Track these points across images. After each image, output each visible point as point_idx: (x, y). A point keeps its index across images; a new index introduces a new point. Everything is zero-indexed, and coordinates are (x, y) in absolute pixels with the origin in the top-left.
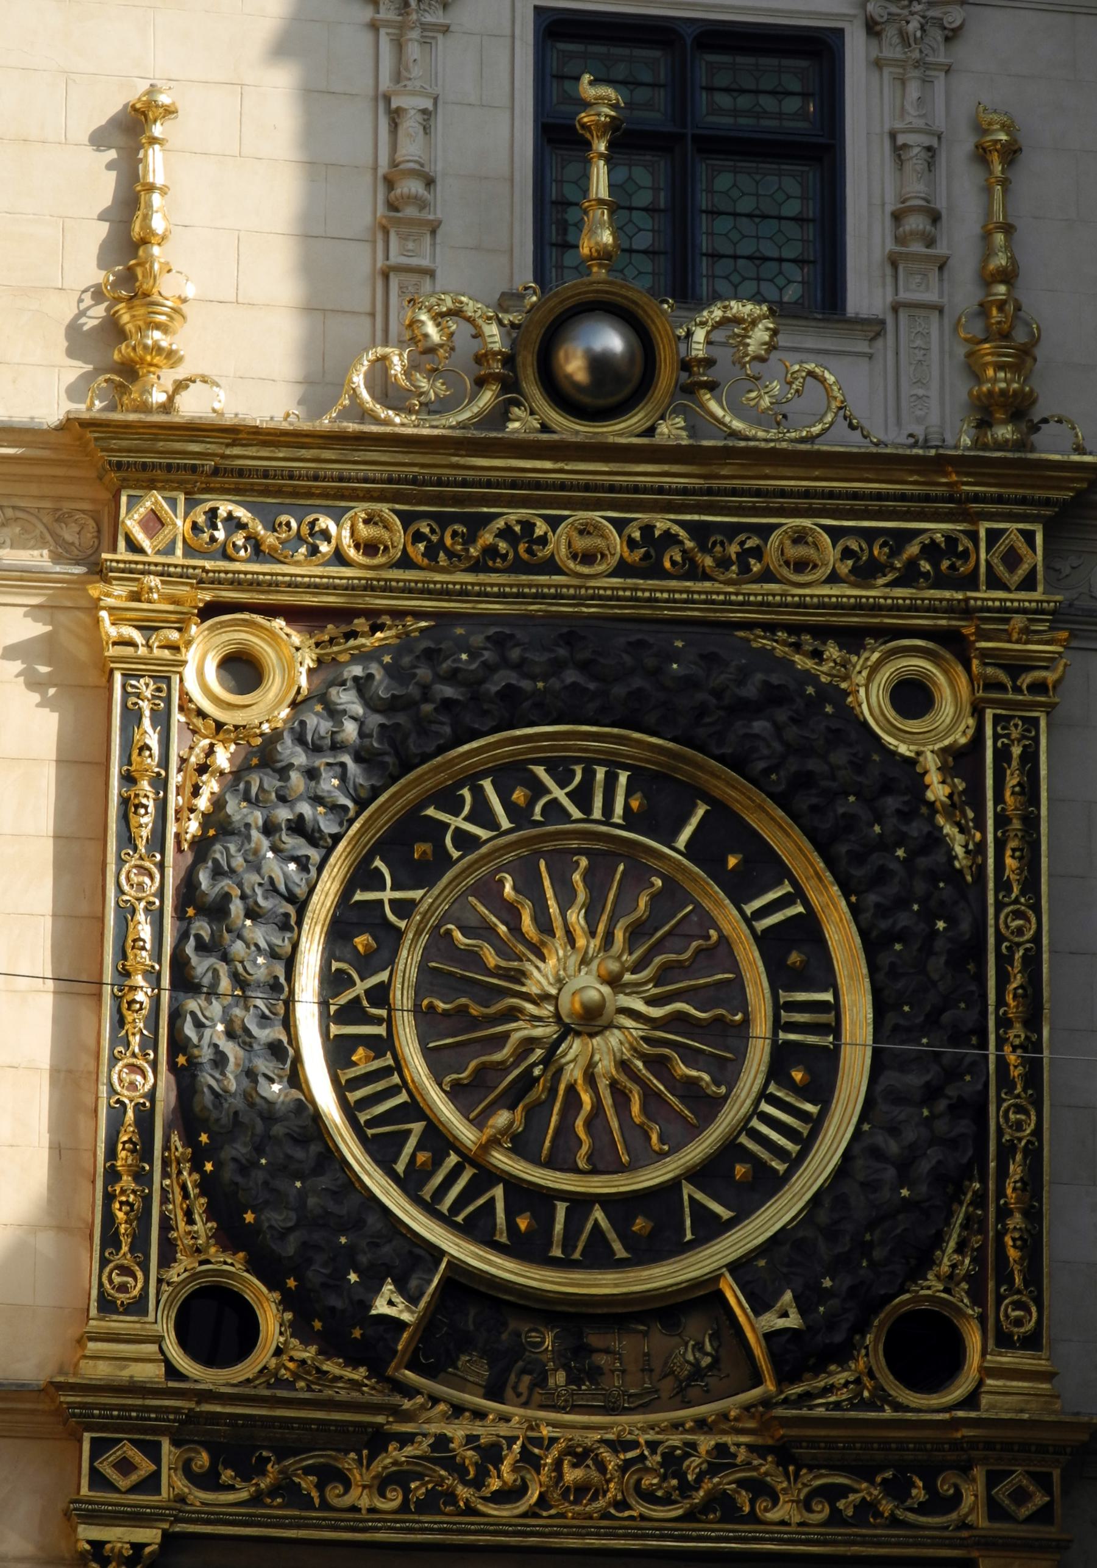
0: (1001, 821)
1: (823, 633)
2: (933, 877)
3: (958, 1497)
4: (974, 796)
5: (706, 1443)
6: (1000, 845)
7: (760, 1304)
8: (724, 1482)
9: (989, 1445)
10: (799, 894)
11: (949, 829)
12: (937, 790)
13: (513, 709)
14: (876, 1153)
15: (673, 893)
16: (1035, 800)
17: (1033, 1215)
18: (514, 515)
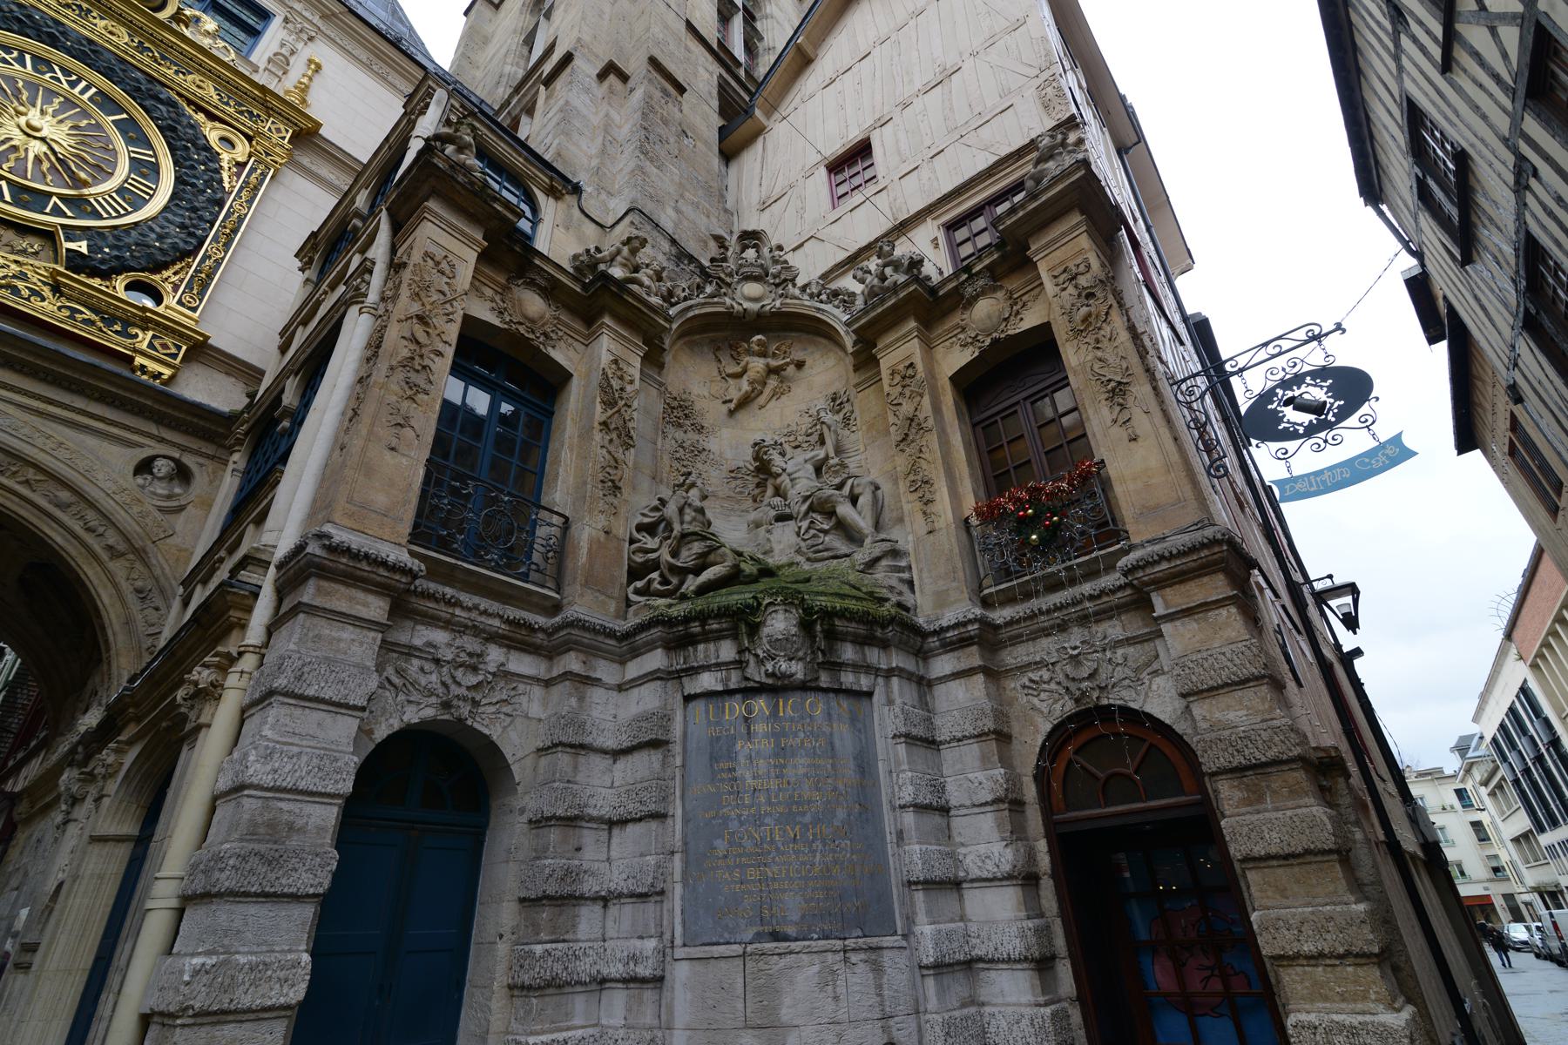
0: (246, 182)
1: (199, 109)
2: (212, 179)
3: (136, 336)
4: (238, 175)
5: (13, 266)
6: (242, 188)
7: (68, 239)
8: (20, 284)
9: (158, 324)
10: (155, 156)
11: (225, 175)
12: (225, 165)
13: (53, 41)
14: (151, 229)
15: (98, 126)
16: (261, 184)
17: (210, 277)
18: (85, 6)
